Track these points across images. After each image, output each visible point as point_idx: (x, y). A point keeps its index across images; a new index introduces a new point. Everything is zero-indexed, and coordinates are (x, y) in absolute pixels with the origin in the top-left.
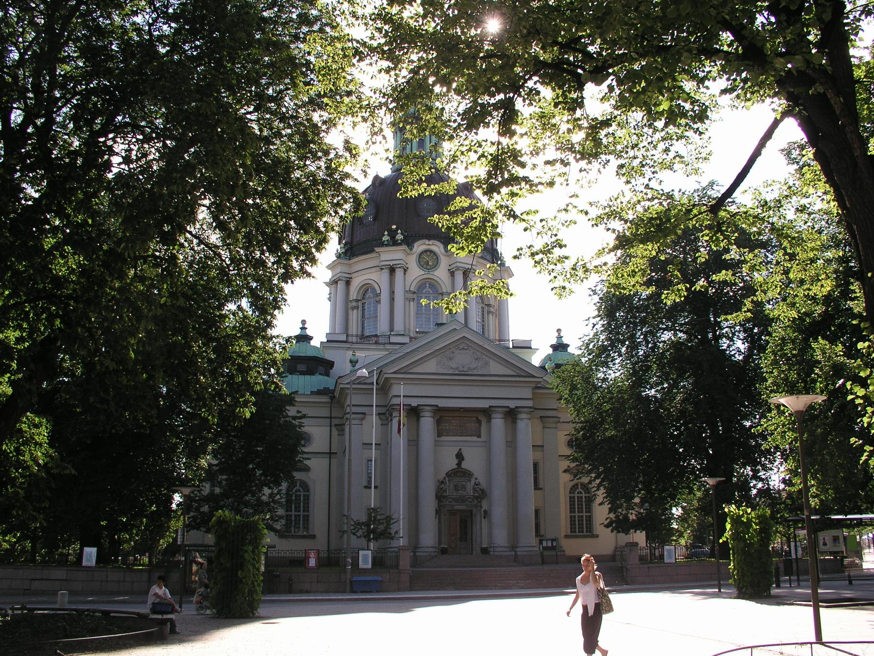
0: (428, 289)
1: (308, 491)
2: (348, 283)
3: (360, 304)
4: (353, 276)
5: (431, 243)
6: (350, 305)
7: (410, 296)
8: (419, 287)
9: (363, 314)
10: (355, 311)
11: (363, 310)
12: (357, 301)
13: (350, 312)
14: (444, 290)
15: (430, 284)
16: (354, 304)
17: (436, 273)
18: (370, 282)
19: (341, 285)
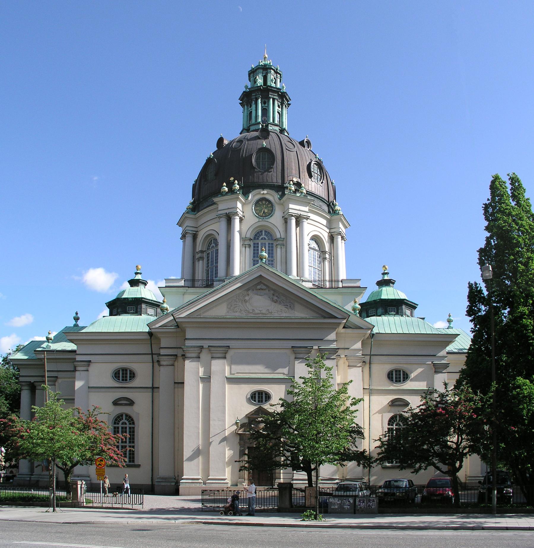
0: (263, 236)
1: (134, 423)
2: (195, 237)
3: (205, 255)
4: (199, 229)
5: (265, 192)
6: (197, 256)
7: (247, 242)
8: (256, 235)
9: (208, 263)
10: (201, 262)
11: (208, 260)
12: (202, 252)
13: (197, 263)
14: (278, 236)
15: (265, 231)
16: (199, 255)
17: (270, 220)
18: (211, 232)
19: (189, 239)
